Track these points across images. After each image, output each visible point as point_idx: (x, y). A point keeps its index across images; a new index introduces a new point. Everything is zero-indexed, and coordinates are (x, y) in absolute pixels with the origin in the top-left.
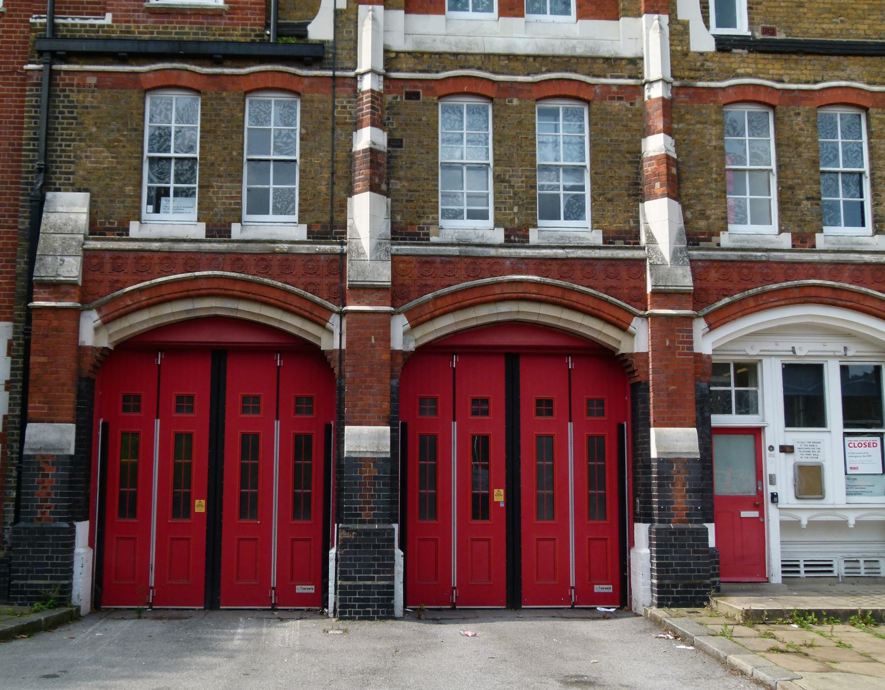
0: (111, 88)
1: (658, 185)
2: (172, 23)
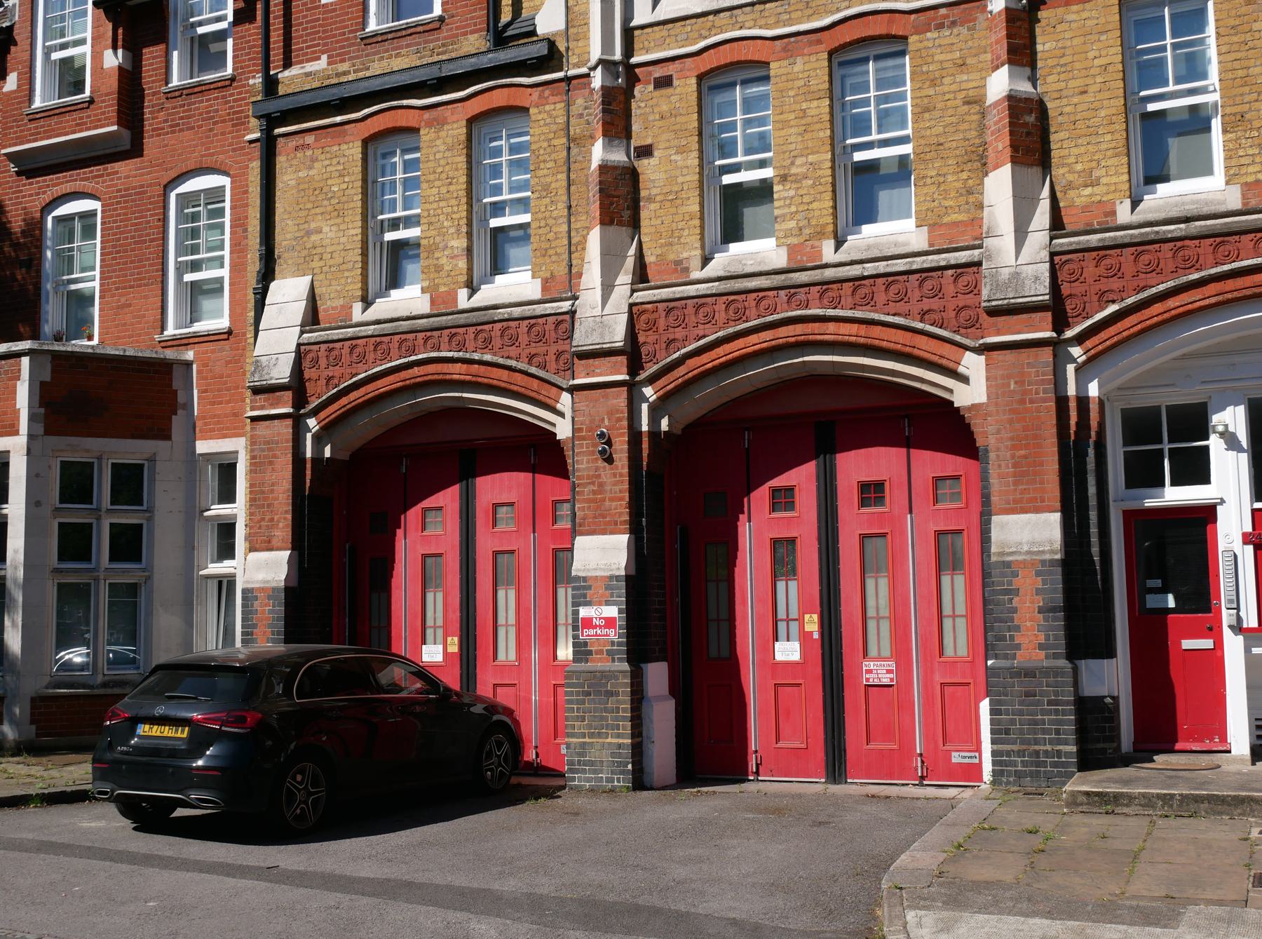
2: (387, 51)
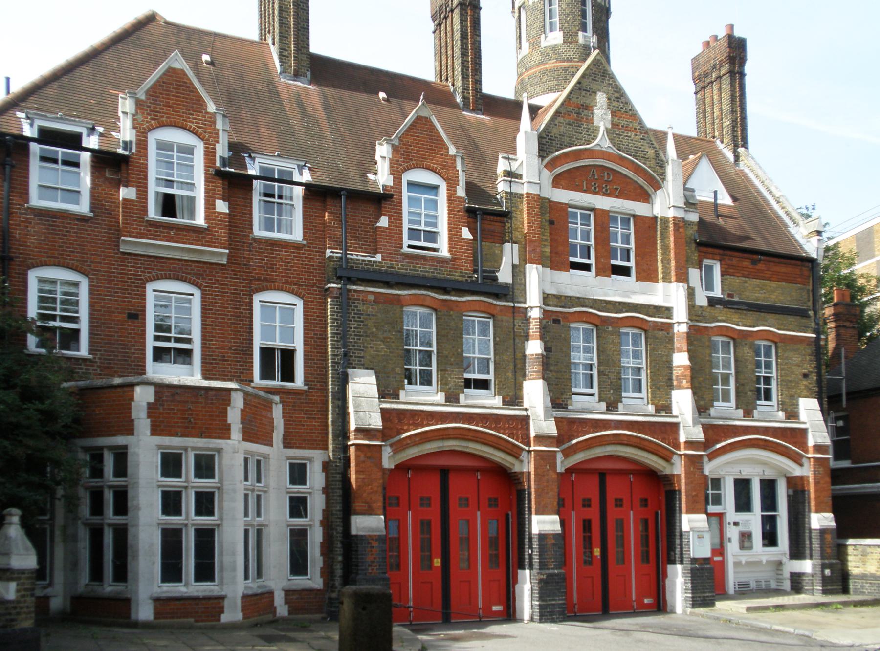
0: (384, 303)
1: (684, 382)
